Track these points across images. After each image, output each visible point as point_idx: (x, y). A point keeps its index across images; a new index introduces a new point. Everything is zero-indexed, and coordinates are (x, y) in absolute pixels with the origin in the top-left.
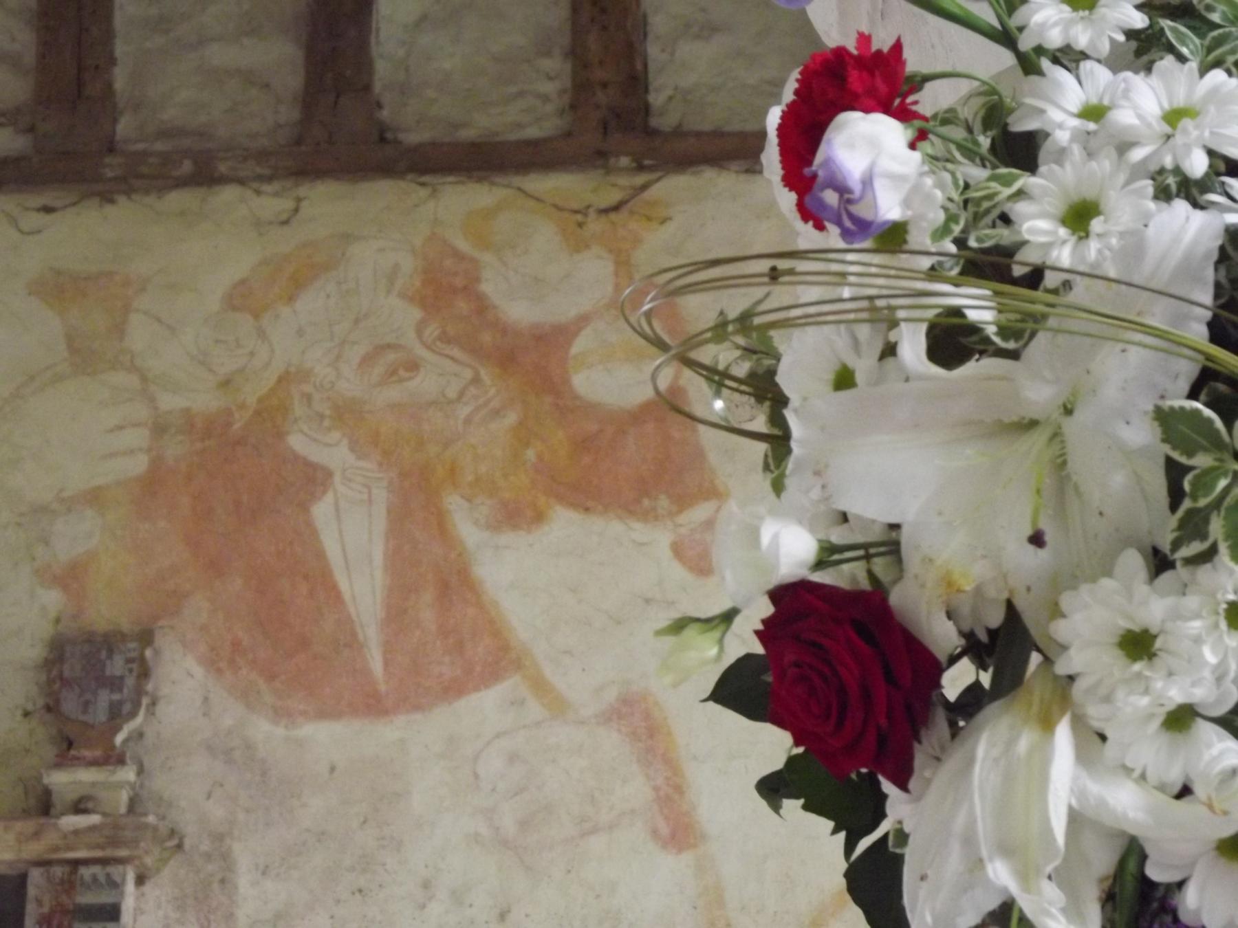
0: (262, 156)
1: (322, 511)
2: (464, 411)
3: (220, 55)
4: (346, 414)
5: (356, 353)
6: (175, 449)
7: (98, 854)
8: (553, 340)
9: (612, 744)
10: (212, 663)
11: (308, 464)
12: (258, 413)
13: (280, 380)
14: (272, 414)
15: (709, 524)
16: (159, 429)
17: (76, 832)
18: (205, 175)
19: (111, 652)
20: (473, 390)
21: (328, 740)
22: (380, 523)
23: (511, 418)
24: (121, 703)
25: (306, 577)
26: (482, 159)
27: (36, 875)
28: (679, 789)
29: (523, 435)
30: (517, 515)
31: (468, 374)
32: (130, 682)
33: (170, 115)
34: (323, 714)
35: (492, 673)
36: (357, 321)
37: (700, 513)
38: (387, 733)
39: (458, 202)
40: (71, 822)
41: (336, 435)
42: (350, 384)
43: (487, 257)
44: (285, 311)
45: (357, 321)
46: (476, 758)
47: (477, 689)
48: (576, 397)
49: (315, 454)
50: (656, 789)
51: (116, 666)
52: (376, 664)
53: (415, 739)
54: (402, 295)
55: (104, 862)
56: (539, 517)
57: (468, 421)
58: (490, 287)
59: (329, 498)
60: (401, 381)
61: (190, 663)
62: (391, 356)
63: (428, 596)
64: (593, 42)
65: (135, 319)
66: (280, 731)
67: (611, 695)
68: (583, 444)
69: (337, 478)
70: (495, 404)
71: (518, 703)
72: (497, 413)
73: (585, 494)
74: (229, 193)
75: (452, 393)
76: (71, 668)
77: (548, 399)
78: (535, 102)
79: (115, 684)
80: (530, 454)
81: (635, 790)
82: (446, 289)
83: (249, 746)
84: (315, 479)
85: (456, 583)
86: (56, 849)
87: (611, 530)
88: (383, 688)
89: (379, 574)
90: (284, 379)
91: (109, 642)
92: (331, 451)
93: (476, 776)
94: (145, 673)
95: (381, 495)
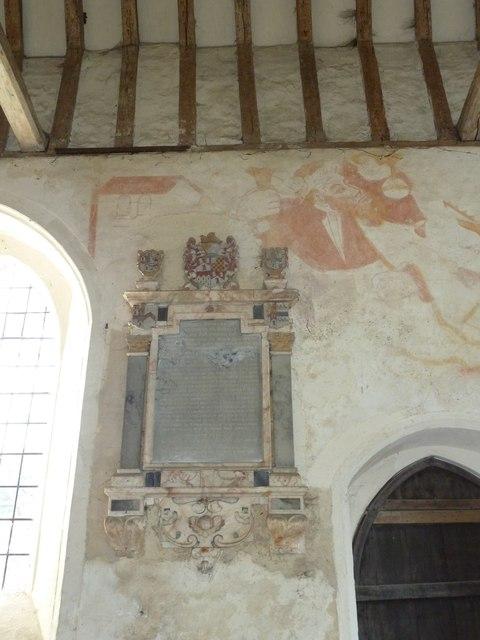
0: (299, 144)
1: (325, 222)
3: (282, 124)
4: (328, 199)
10: (301, 257)
13: (311, 192)
14: (310, 200)
15: (423, 226)
16: (282, 202)
18: (285, 147)
21: (334, 275)
22: (340, 226)
23: (370, 201)
26: (353, 145)
29: (373, 205)
30: (375, 223)
33: (272, 137)
34: (330, 269)
35: (372, 262)
37: (421, 222)
38: (349, 273)
39: (350, 153)
42: (329, 193)
43: (359, 166)
49: (323, 209)
53: (356, 274)
55: (283, 301)
58: (361, 172)
61: (295, 256)
67: (404, 265)
71: (381, 267)
73: (392, 219)
74: (293, 151)
78: (365, 133)
81: (413, 287)
82: (349, 173)
83: (313, 276)
84: (322, 214)
85: (361, 238)
91: (277, 250)
92: (326, 208)
95: (339, 219)
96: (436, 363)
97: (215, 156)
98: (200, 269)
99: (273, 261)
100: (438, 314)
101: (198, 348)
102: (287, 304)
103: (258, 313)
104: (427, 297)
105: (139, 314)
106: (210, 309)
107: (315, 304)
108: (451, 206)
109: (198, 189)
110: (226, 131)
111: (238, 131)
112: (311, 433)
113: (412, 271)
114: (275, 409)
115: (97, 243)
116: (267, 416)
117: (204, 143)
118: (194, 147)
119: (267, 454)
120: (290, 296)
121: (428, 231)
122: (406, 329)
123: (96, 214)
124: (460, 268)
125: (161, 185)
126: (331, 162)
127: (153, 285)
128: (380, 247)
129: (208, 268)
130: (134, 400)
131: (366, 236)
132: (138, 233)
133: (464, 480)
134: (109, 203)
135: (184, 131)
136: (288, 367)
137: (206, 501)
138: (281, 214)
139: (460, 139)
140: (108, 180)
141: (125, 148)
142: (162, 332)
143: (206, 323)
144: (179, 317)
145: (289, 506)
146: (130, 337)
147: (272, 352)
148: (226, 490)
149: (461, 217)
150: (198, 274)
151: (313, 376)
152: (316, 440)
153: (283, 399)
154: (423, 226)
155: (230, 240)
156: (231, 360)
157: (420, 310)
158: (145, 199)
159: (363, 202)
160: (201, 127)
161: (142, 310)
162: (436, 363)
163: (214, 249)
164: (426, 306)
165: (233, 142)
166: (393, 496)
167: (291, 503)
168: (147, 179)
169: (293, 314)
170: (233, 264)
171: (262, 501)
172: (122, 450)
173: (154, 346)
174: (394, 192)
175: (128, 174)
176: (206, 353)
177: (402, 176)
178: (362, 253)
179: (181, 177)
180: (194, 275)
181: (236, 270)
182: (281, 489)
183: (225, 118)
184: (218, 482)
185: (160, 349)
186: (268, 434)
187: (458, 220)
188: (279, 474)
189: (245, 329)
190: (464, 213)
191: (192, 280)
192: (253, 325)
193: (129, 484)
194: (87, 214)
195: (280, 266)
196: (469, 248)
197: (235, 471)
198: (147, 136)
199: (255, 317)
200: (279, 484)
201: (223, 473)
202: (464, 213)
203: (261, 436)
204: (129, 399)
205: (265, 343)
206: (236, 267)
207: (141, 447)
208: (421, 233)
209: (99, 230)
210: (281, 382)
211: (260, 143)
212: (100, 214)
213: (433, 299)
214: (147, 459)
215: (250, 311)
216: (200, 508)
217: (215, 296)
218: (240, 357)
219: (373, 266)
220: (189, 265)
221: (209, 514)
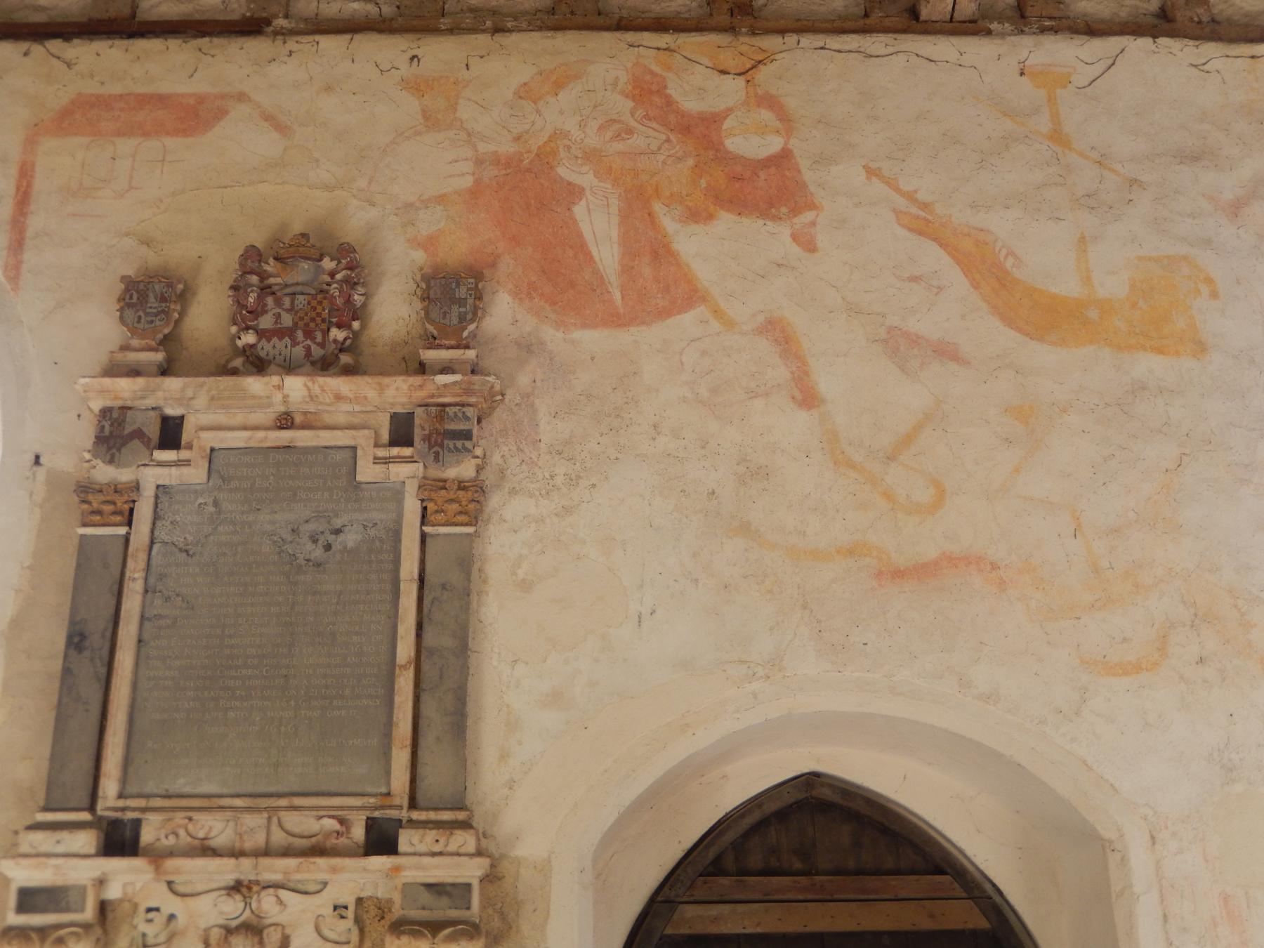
1: (579, 210)
2: (662, 158)
4: (592, 156)
5: (594, 125)
7: (457, 399)
8: (713, 120)
10: (516, 295)
11: (569, 184)
12: (538, 155)
14: (545, 159)
15: (813, 224)
16: (479, 162)
17: (445, 386)
19: (458, 285)
20: (666, 145)
21: (592, 339)
22: (615, 220)
23: (691, 162)
24: (466, 313)
25: (571, 247)
26: (660, 25)
27: (419, 412)
28: (806, 373)
30: (695, 216)
31: (664, 137)
32: (470, 301)
34: (584, 326)
36: (595, 107)
37: (809, 216)
40: (442, 379)
41: (585, 169)
42: (593, 141)
43: (670, 76)
44: (552, 100)
45: (595, 107)
46: (681, 354)
47: (679, 313)
48: (729, 152)
50: (792, 373)
51: (462, 292)
52: (617, 296)
54: (623, 93)
56: (711, 217)
57: (664, 163)
59: (583, 203)
60: (623, 139)
62: (617, 126)
65: (461, 101)
66: (560, 335)
67: (761, 319)
69: (588, 192)
70: (680, 154)
73: (740, 204)
74: (515, 37)
75: (654, 147)
77: (711, 153)
79: (461, 302)
80: (703, 183)
81: (779, 372)
82: (647, 92)
84: (574, 192)
85: (662, 252)
86: (433, 396)
87: (752, 225)
88: (622, 311)
89: (616, 246)
90: (554, 136)
92: (584, 177)
93: (682, 363)
94: (479, 298)
95: (614, 202)
97: (329, 43)
98: (266, 322)
99: (452, 296)
101: (251, 518)
103: (401, 432)
104: (808, 398)
105: (114, 434)
106: (285, 421)
113: (778, 332)
118: (280, 22)
119: (399, 780)
121: (822, 239)
123: (29, 185)
124: (890, 330)
125: (193, 116)
128: (704, 273)
129: (287, 320)
130: (87, 646)
131: (676, 246)
132: (127, 234)
133: (885, 830)
134: (61, 159)
136: (466, 562)
137: (249, 889)
138: (475, 193)
139: (914, 13)
144: (210, 439)
145: (445, 901)
146: (85, 489)
147: (427, 529)
149: (901, 202)
150: (261, 334)
151: (526, 586)
152: (520, 743)
153: (447, 641)
154: (813, 224)
156: (328, 547)
157: (795, 426)
158: (154, 144)
164: (803, 419)
166: (716, 869)
167: (450, 895)
168: (162, 100)
172: (51, 768)
173: (144, 511)
174: (749, 141)
175: (116, 89)
176: (269, 528)
177: (771, 102)
178: (663, 288)
179: (242, 97)
185: (156, 517)
187: (894, 211)
188: (424, 824)
189: (367, 472)
190: (910, 197)
192: (387, 461)
193: (60, 849)
196: (915, 279)
197: (321, 817)
199: (393, 443)
200: (422, 848)
203: (388, 735)
204: (76, 640)
205: (412, 507)
208: (810, 247)
209: (35, 223)
210: (447, 601)
212: (40, 184)
213: (823, 401)
214: (109, 787)
216: (233, 908)
218: (351, 538)
219: (688, 321)
221: (254, 921)
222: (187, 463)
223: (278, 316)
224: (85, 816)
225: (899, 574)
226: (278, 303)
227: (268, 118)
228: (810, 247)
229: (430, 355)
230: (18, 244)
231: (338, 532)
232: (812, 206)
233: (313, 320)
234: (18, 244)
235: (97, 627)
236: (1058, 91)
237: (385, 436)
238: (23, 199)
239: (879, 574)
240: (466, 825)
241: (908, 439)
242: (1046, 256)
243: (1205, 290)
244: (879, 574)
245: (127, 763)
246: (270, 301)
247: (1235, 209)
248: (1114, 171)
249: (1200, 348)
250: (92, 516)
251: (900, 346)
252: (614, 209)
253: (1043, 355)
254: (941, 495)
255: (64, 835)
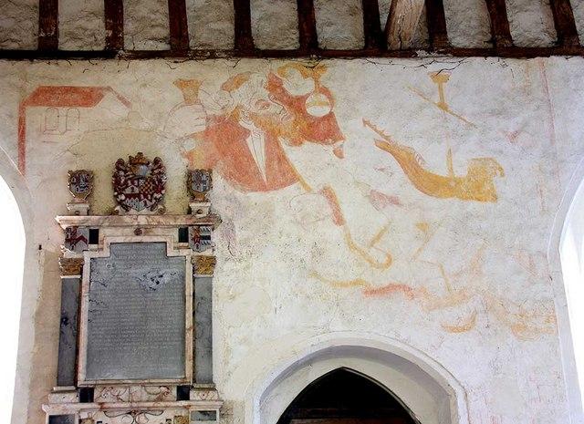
0: (226, 52)
1: (249, 140)
3: (213, 26)
4: (253, 116)
5: (254, 102)
6: (212, 124)
8: (301, 99)
9: (322, 199)
14: (235, 116)
16: (208, 119)
18: (213, 55)
21: (255, 197)
22: (263, 144)
23: (293, 119)
29: (296, 122)
30: (297, 143)
33: (202, 40)
34: (252, 191)
39: (276, 64)
42: (253, 109)
49: (246, 126)
51: (204, 178)
53: (276, 196)
55: (206, 225)
63: (276, 162)
64: (305, 27)
67: (321, 187)
68: (310, 125)
72: (289, 117)
74: (220, 61)
76: (193, 178)
78: (291, 41)
79: (204, 182)
81: (329, 210)
82: (275, 86)
84: (247, 132)
85: (282, 159)
91: (201, 172)
92: (250, 126)
95: (263, 137)
96: (344, 285)
98: (128, 191)
100: (348, 236)
102: (209, 228)
103: (183, 236)
104: (339, 221)
105: (72, 238)
106: (138, 232)
107: (237, 226)
108: (370, 126)
109: (127, 103)
110: (154, 32)
111: (165, 32)
112: (228, 351)
113: (328, 194)
114: (197, 329)
115: (26, 160)
116: (189, 336)
117: (131, 48)
119: (189, 372)
120: (213, 219)
121: (347, 152)
122: (318, 252)
123: (24, 128)
125: (89, 97)
126: (258, 72)
127: (83, 207)
128: (298, 167)
129: (137, 190)
130: (69, 321)
134: (37, 115)
135: (110, 33)
136: (210, 289)
138: (207, 133)
140: (34, 89)
141: (48, 50)
142: (96, 255)
143: (138, 246)
146: (63, 260)
148: (151, 404)
149: (378, 137)
150: (127, 196)
151: (233, 298)
153: (204, 319)
155: (157, 161)
156: (158, 283)
157: (335, 232)
159: (286, 119)
160: (129, 26)
161: (74, 233)
162: (344, 285)
163: (143, 170)
165: (163, 47)
168: (74, 90)
169: (216, 236)
170: (159, 186)
171: (184, 413)
172: (58, 370)
173: (86, 269)
174: (316, 110)
175: (55, 84)
177: (325, 91)
178: (283, 175)
179: (109, 89)
180: (123, 197)
181: (163, 192)
182: (202, 403)
183: (153, 16)
184: (145, 397)
185: (92, 271)
186: (189, 353)
189: (171, 253)
190: (381, 134)
191: (120, 203)
192: (179, 248)
193: (65, 400)
194: (15, 128)
195: (205, 190)
196: (382, 170)
198: (74, 37)
200: (198, 398)
201: (149, 389)
202: (381, 134)
203: (183, 355)
204: (64, 320)
206: (163, 188)
207: (76, 366)
208: (341, 156)
209: (28, 146)
210: (203, 304)
211: (189, 49)
212: (28, 128)
214: (81, 377)
215: (175, 234)
217: (142, 221)
218: (166, 279)
219: (292, 187)
220: (118, 186)
222: (102, 249)
223: (133, 188)
224: (73, 388)
225: (373, 292)
226: (133, 183)
227: (121, 98)
228: (341, 156)
229: (195, 206)
230: (22, 155)
231: (162, 276)
232: (342, 138)
233: (147, 190)
234: (22, 155)
235: (71, 315)
236: (444, 84)
237: (177, 240)
238: (22, 134)
239: (366, 292)
240: (214, 389)
241: (379, 237)
242: (435, 163)
243: (499, 173)
244: (366, 292)
245: (88, 367)
246: (129, 182)
247: (514, 135)
248: (465, 120)
249: (495, 198)
250: (67, 271)
251: (376, 198)
252: (263, 140)
253: (432, 202)
254: (389, 263)
255: (67, 395)
